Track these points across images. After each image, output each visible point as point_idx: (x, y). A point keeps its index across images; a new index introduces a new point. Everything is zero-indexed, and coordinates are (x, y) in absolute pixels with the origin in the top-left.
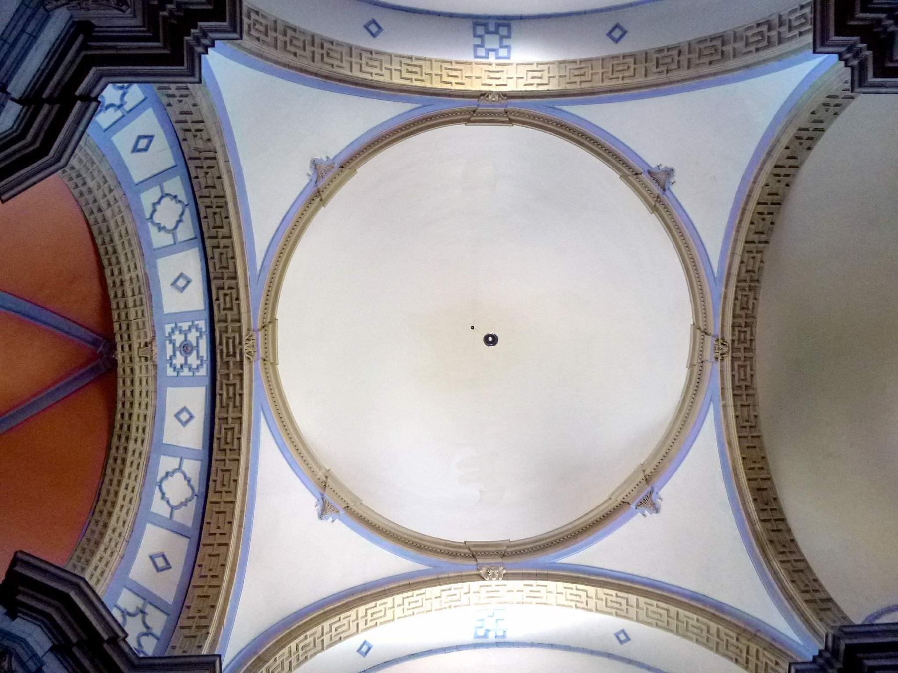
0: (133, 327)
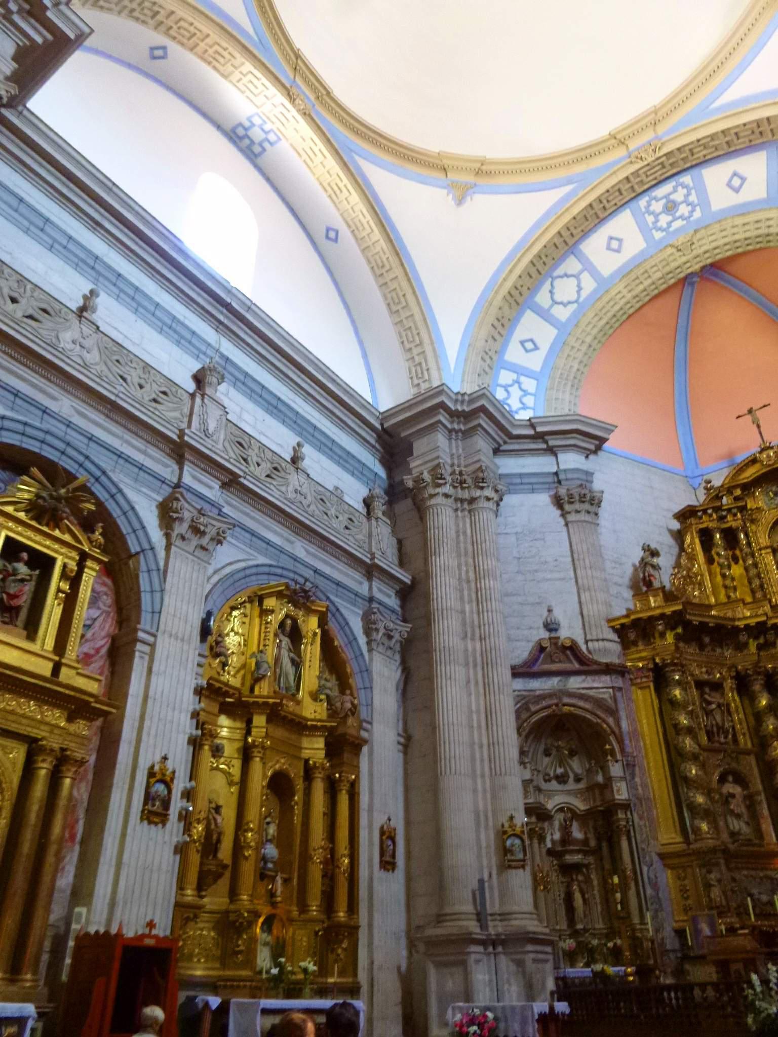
0: (668, 269)
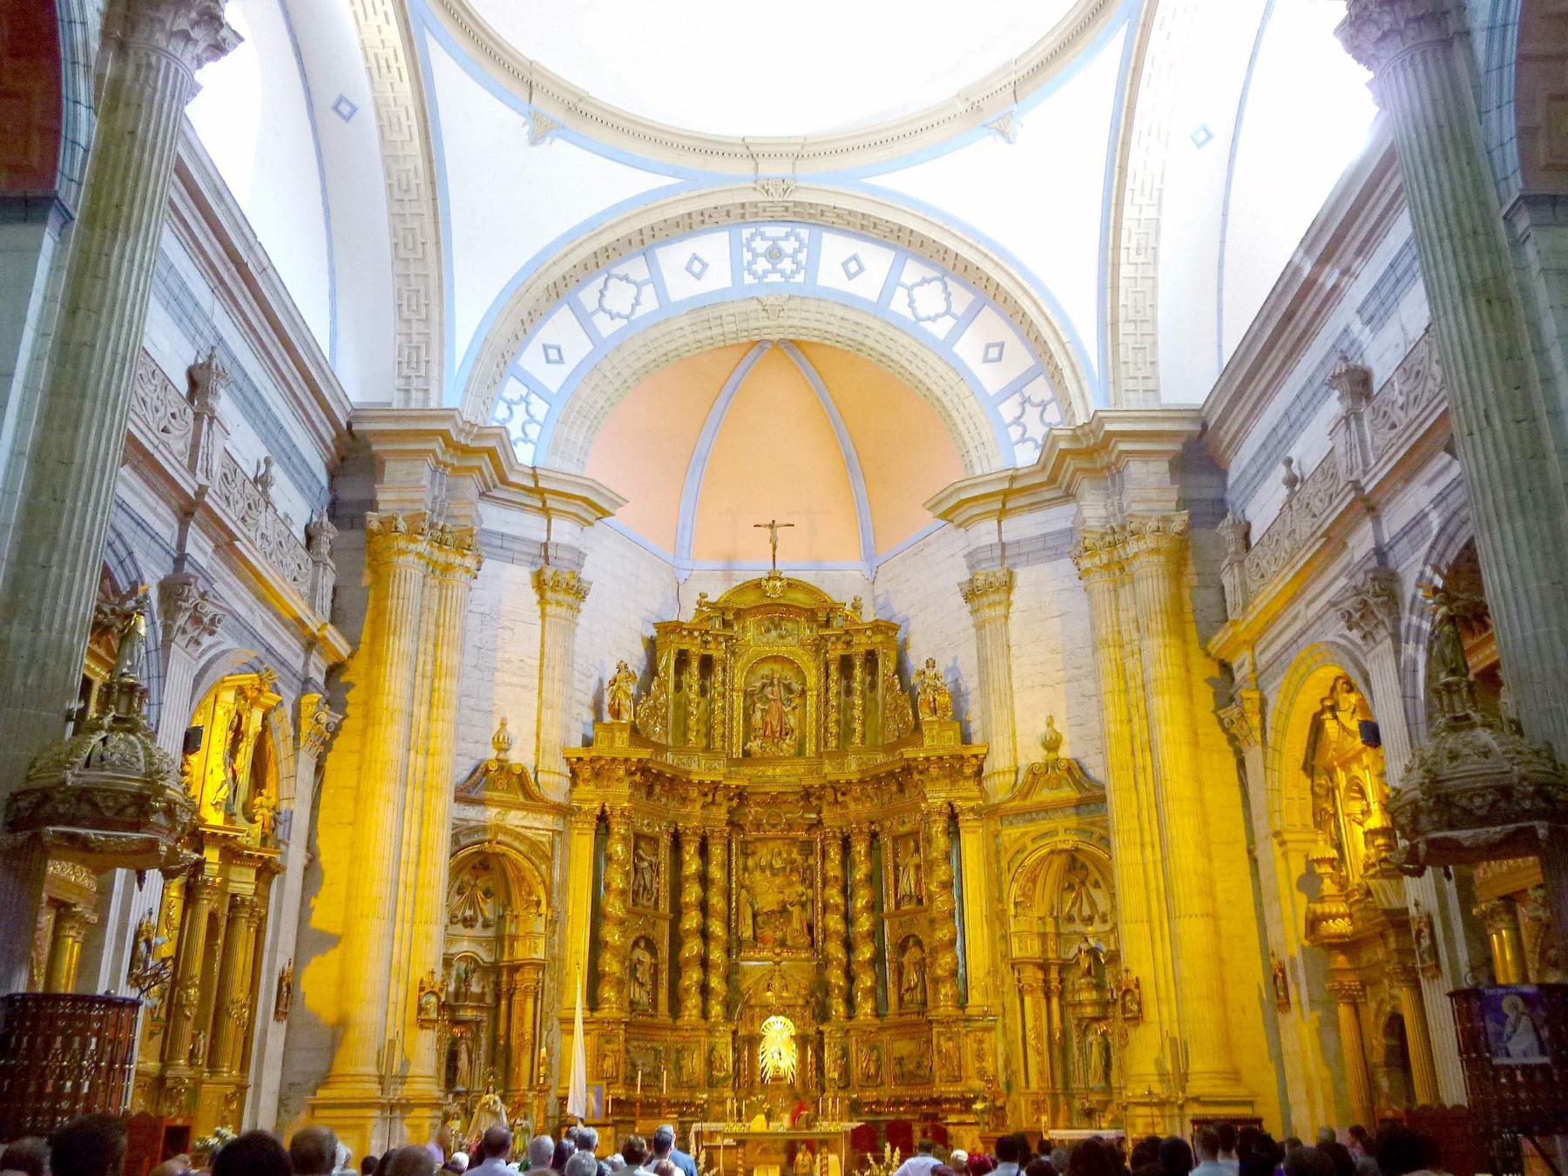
0: (744, 325)
